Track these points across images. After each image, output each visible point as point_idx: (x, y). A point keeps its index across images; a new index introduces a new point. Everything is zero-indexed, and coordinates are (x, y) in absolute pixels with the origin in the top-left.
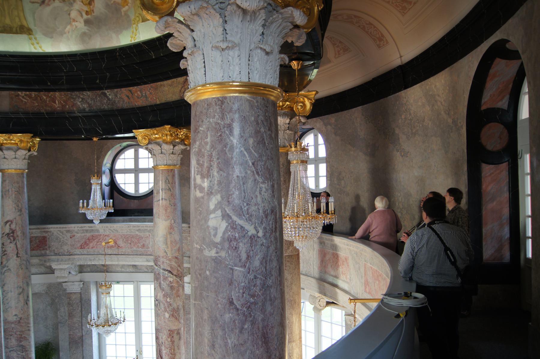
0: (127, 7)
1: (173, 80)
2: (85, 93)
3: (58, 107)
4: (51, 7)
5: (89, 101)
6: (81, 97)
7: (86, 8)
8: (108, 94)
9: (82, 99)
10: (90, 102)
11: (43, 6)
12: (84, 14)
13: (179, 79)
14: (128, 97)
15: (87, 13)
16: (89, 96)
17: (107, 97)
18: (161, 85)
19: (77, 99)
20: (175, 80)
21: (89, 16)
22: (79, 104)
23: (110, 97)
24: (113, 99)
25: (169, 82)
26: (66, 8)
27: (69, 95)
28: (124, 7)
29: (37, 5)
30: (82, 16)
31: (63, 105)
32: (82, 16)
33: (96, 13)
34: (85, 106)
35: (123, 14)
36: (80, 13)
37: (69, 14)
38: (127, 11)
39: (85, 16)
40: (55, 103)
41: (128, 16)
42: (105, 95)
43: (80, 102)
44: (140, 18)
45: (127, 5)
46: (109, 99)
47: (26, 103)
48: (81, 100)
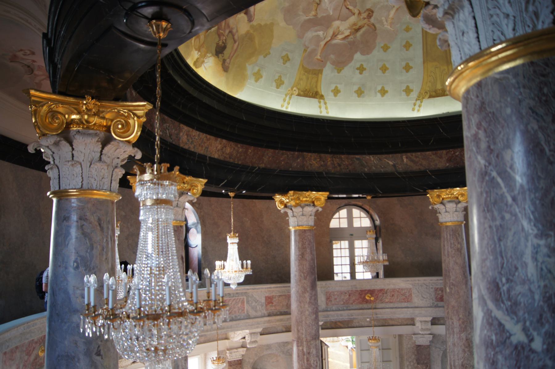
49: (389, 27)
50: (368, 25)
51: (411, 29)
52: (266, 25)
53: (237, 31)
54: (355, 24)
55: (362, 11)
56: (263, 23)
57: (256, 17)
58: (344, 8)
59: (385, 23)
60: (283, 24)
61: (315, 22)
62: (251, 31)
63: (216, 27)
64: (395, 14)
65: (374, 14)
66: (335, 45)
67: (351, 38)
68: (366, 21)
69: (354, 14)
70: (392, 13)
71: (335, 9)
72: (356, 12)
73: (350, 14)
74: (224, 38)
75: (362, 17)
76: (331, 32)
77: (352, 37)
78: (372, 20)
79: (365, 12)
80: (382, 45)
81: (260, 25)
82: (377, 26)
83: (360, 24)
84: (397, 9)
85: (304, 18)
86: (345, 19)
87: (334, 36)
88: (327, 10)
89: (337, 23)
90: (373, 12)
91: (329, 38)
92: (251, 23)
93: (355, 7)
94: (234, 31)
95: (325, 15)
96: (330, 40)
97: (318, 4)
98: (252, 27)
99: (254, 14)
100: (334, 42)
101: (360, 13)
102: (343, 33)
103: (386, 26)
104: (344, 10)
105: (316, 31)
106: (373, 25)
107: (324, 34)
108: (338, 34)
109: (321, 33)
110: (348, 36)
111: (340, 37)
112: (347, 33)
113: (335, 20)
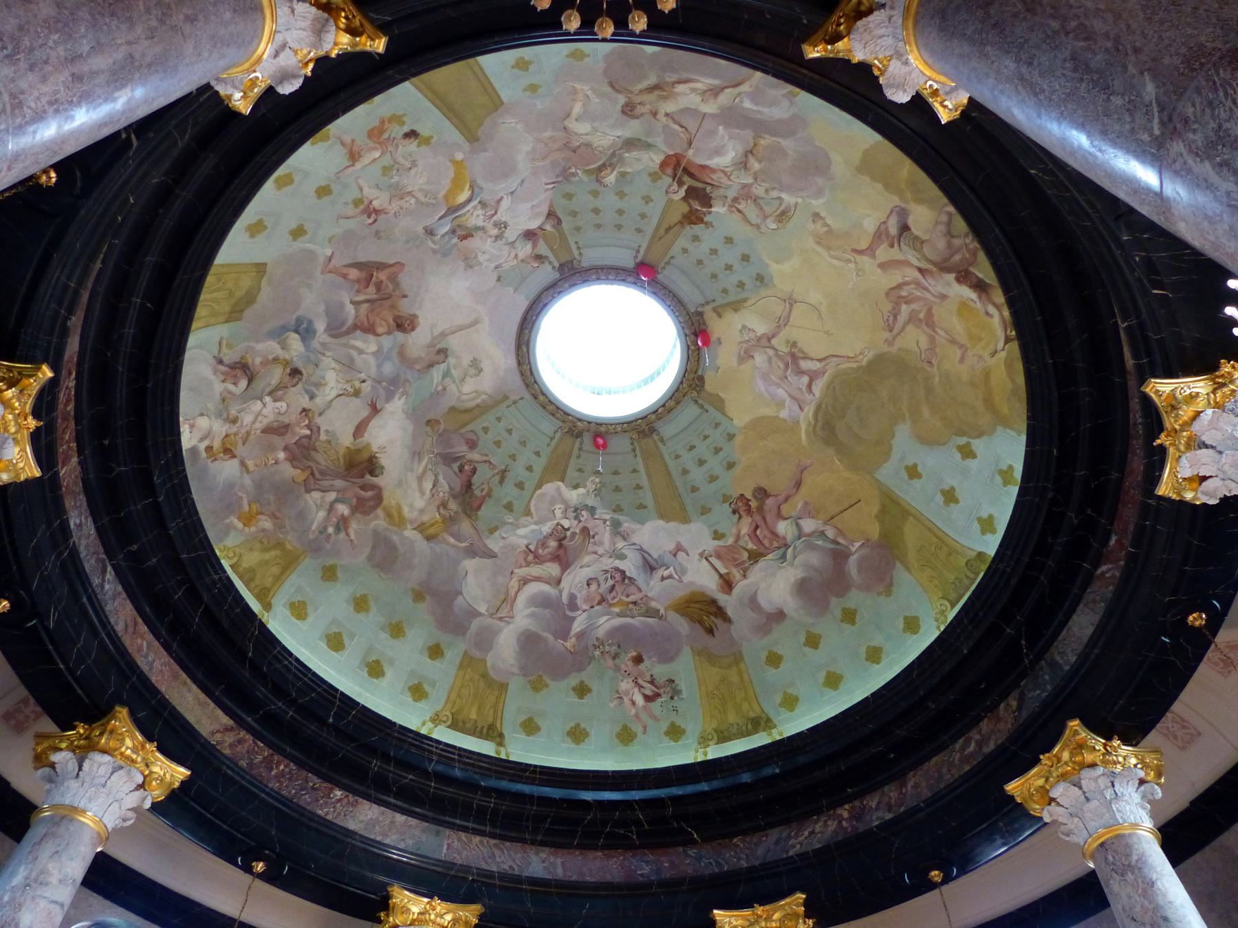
0: (240, 525)
1: (209, 701)
2: (90, 519)
4: (212, 377)
7: (217, 444)
11: (213, 362)
12: (206, 443)
13: (219, 712)
14: (126, 626)
15: (209, 449)
17: (103, 580)
18: (185, 683)
19: (76, 512)
20: (212, 705)
21: (204, 455)
23: (107, 587)
25: (202, 696)
26: (211, 406)
28: (239, 519)
29: (215, 350)
30: (202, 440)
32: (202, 440)
33: (214, 467)
35: (227, 521)
36: (208, 435)
37: (202, 415)
38: (235, 528)
39: (202, 446)
41: (227, 534)
42: (104, 571)
44: (236, 559)
45: (245, 525)
49: (578, 86)
50: (631, 92)
51: (525, 90)
52: (874, 178)
53: (937, 223)
54: (665, 98)
55: (650, 117)
56: (880, 186)
57: (890, 206)
58: (693, 132)
59: (589, 93)
60: (836, 158)
61: (760, 127)
62: (908, 194)
63: (972, 269)
64: (571, 109)
65: (619, 108)
66: (715, 77)
67: (670, 77)
68: (637, 100)
69: (667, 115)
70: (577, 109)
71: (713, 133)
72: (661, 116)
73: (676, 118)
74: (967, 241)
75: (648, 107)
76: (725, 98)
77: (670, 80)
78: (622, 99)
79: (642, 115)
80: (586, 60)
81: (886, 186)
82: (610, 89)
83: (652, 97)
84: (568, 116)
85: (787, 144)
86: (686, 111)
87: (715, 92)
88: (731, 137)
89: (709, 108)
90: (623, 112)
91: (727, 91)
92: (903, 205)
93: (666, 127)
94: (942, 228)
95: (737, 131)
96: (727, 87)
97: (751, 152)
98: (901, 197)
99: (892, 212)
100: (716, 82)
101: (655, 114)
102: (694, 90)
103: (586, 88)
104: (692, 127)
105: (759, 112)
106: (618, 91)
107: (742, 102)
108: (705, 92)
109: (747, 104)
110: (679, 82)
111: (698, 85)
112: (680, 88)
113: (712, 116)
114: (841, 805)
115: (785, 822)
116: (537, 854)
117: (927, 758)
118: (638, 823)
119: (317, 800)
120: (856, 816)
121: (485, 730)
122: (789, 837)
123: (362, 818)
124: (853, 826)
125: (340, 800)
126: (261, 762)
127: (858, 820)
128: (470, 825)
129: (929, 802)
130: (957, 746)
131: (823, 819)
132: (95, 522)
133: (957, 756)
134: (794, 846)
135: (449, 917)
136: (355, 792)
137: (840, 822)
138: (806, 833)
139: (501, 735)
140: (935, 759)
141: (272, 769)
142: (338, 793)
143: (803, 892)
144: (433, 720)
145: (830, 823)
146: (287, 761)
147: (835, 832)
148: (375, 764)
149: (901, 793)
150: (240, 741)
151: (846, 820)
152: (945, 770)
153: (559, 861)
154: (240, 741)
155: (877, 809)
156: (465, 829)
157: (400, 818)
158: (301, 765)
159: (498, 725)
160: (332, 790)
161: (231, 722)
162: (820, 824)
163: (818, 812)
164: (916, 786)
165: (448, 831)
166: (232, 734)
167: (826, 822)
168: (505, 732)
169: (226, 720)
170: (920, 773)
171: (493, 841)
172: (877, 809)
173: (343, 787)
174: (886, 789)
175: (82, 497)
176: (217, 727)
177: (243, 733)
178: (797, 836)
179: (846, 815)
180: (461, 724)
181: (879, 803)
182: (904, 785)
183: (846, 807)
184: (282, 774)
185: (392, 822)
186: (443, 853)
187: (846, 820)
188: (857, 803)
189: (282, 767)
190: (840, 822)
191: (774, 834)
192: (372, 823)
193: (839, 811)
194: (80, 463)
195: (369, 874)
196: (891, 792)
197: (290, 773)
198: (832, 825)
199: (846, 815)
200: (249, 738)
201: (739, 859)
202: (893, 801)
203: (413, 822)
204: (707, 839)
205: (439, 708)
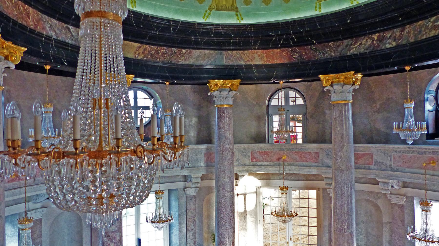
3: (32, 25)
5: (56, 29)
6: (50, 23)
8: (72, 30)
9: (51, 25)
10: (57, 32)
16: (56, 25)
17: (71, 33)
19: (46, 23)
22: (48, 29)
24: (76, 37)
27: (40, 16)
31: (35, 25)
34: (53, 34)
40: (30, 19)
42: (69, 29)
43: (49, 27)
46: (72, 35)
47: (8, 7)
48: (49, 25)
114: (374, 33)
115: (351, 37)
116: (257, 53)
117: (417, 21)
118: (292, 39)
119: (178, 57)
120: (381, 40)
121: (230, 7)
122: (352, 44)
123: (194, 57)
124: (378, 44)
125: (185, 53)
126: (155, 53)
127: (380, 41)
128: (231, 48)
129: (412, 44)
130: (432, 19)
131: (366, 38)
132: (54, 18)
133: (431, 24)
134: (353, 48)
135: (230, 84)
136: (189, 48)
137: (373, 41)
138: (358, 44)
139: (237, 8)
140: (420, 22)
141: (159, 53)
142: (184, 51)
143: (353, 71)
144: (209, 9)
145: (369, 40)
146: (163, 48)
147: (370, 46)
148: (193, 38)
149: (401, 33)
150: (145, 49)
151: (376, 40)
152: (423, 29)
153: (265, 55)
154: (145, 49)
155: (390, 38)
156: (230, 50)
157: (207, 52)
158: (168, 46)
159: (235, 4)
160: (181, 51)
161: (139, 44)
162: (365, 40)
163: (365, 35)
164: (409, 32)
165: (224, 52)
166: (141, 48)
167: (367, 40)
168: (238, 6)
169: (137, 45)
170: (412, 27)
171: (240, 52)
172: (390, 38)
173: (184, 48)
174: (395, 30)
175: (45, 16)
176: (135, 49)
177: (145, 46)
178: (355, 44)
179: (376, 38)
180: (220, 8)
181: (391, 36)
182: (403, 30)
183: (377, 35)
184: (163, 53)
185: (205, 54)
186: (225, 62)
187: (376, 40)
188: (382, 34)
189: (162, 51)
190: (373, 41)
191: (346, 42)
192: (198, 58)
193: (373, 36)
194: (33, 8)
195: (202, 76)
196: (397, 32)
197: (165, 51)
198: (370, 42)
199: (376, 38)
200: (147, 46)
201: (331, 52)
202: (397, 37)
203: (212, 52)
204: (319, 43)
205: (210, 4)
